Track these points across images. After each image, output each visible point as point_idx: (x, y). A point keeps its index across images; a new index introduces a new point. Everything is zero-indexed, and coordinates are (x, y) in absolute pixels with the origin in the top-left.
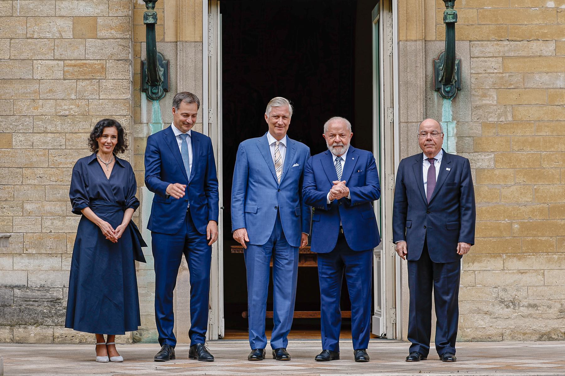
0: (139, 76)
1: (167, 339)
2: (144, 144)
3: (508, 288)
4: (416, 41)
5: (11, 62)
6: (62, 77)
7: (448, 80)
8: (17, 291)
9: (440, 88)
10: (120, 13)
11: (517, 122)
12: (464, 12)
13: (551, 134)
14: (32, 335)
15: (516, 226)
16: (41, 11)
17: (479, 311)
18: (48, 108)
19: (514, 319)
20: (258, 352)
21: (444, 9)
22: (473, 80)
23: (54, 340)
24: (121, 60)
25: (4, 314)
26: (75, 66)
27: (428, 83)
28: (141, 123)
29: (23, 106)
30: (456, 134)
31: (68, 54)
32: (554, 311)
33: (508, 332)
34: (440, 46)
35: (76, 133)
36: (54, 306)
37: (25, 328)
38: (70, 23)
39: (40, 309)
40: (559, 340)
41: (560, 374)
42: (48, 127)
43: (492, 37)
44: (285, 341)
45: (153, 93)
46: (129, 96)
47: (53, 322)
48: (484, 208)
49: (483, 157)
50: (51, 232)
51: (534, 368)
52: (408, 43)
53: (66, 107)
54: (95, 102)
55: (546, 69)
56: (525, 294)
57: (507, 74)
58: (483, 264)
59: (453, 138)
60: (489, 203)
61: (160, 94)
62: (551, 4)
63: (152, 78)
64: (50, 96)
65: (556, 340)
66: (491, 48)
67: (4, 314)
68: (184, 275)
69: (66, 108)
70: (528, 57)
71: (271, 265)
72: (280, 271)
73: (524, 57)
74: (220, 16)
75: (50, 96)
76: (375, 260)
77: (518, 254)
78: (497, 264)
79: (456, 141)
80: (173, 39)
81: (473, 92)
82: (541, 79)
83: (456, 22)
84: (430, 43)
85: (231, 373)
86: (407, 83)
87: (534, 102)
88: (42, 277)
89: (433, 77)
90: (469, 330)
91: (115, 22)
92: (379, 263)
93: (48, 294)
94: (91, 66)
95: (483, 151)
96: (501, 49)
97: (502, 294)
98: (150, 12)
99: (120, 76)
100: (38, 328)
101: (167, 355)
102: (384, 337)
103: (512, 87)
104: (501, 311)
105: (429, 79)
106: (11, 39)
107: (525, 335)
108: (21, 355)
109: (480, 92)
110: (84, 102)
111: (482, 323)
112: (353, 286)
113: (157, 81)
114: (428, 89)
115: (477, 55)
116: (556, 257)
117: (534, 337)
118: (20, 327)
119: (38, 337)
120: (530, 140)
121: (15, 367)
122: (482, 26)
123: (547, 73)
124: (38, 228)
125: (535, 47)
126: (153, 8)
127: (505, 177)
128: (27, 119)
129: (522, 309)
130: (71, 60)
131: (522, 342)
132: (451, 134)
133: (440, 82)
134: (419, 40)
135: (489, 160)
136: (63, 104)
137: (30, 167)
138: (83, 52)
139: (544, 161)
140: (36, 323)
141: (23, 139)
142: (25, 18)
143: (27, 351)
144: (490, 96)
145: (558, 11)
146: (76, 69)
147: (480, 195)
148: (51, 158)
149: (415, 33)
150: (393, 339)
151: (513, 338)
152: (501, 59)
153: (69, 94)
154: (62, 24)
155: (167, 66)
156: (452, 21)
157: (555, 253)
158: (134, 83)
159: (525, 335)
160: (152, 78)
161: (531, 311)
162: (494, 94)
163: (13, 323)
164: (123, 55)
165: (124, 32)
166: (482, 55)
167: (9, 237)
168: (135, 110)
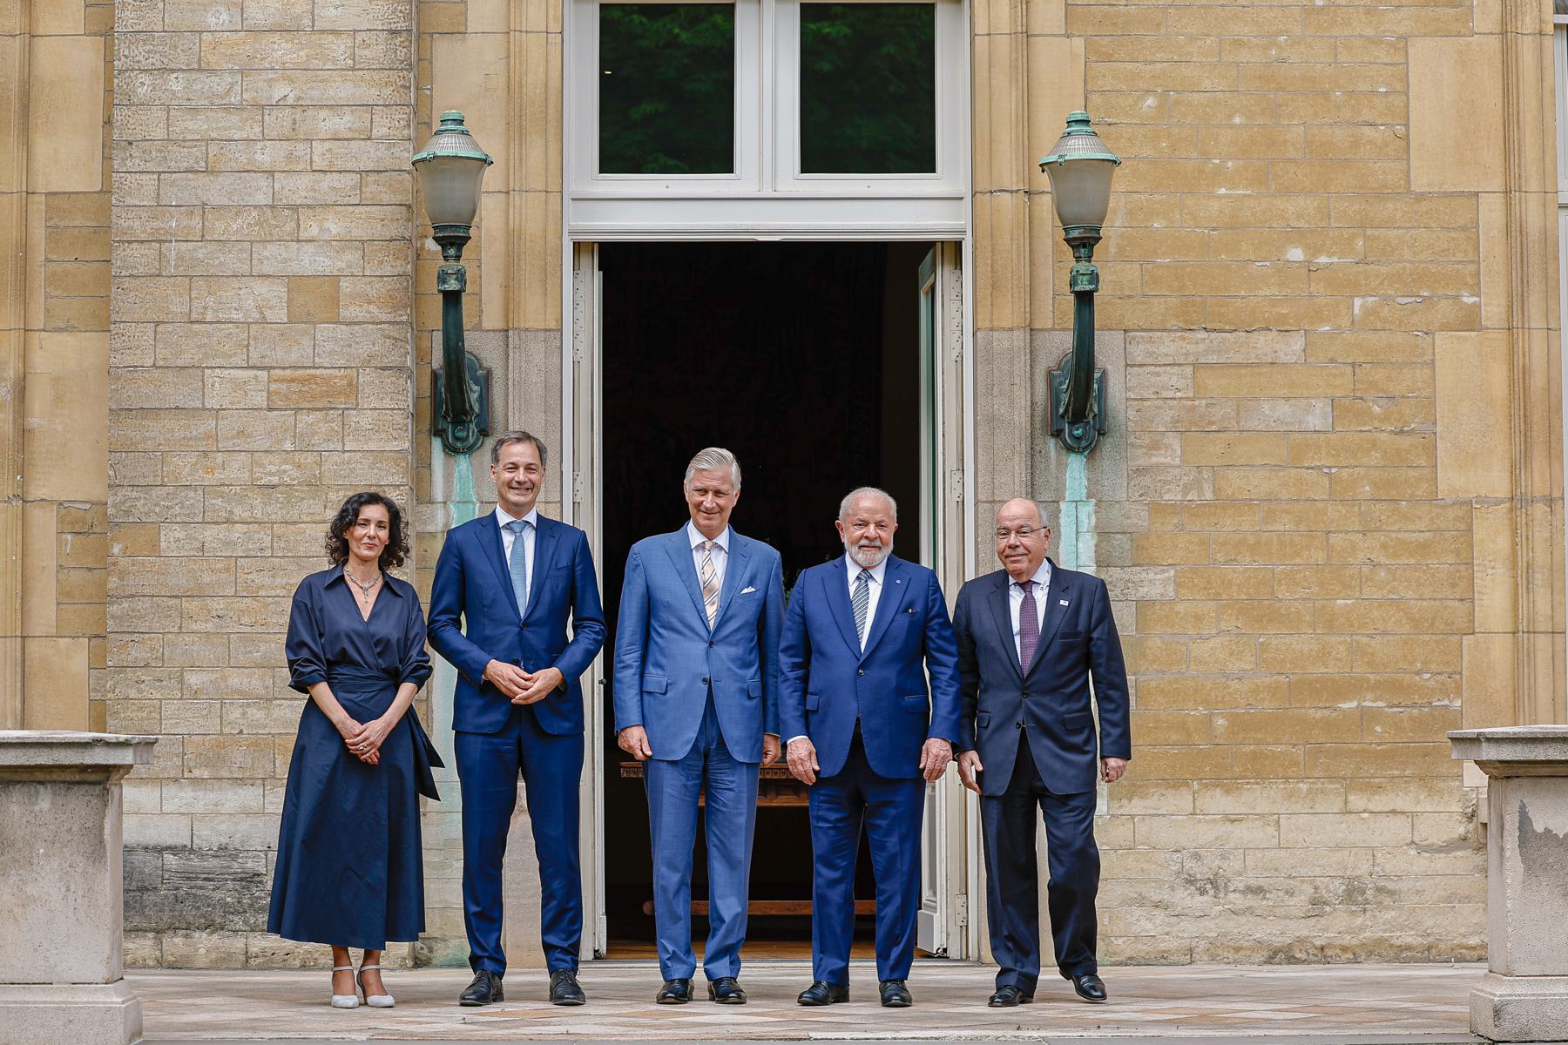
0: (428, 401)
1: (488, 960)
2: (438, 546)
3: (1202, 852)
4: (1011, 329)
5: (156, 373)
6: (264, 405)
7: (1078, 414)
8: (169, 858)
9: (1062, 431)
10: (388, 270)
11: (1224, 503)
12: (1114, 271)
13: (1293, 527)
14: (202, 951)
15: (1221, 721)
16: (221, 264)
17: (1141, 901)
18: (236, 470)
19: (1216, 917)
20: (677, 985)
21: (1072, 262)
22: (1131, 413)
23: (247, 962)
24: (390, 368)
25: (143, 907)
26: (292, 380)
27: (1038, 419)
28: (431, 502)
29: (183, 465)
30: (1096, 527)
31: (280, 355)
32: (1299, 902)
33: (1203, 944)
34: (1063, 342)
35: (294, 523)
36: (248, 889)
37: (186, 936)
38: (281, 290)
39: (217, 895)
40: (1310, 963)
41: (1312, 1033)
42: (236, 511)
43: (1172, 323)
44: (735, 963)
45: (458, 439)
46: (407, 445)
47: (246, 922)
48: (1153, 684)
49: (1151, 575)
50: (241, 732)
51: (1257, 1020)
52: (996, 334)
53: (273, 469)
54: (335, 457)
55: (1284, 392)
56: (1237, 865)
57: (1204, 402)
58: (1148, 802)
59: (1088, 536)
60: (1164, 672)
61: (471, 440)
62: (1296, 254)
63: (455, 406)
64: (240, 443)
65: (1304, 962)
66: (1169, 346)
67: (143, 907)
68: (521, 824)
69: (272, 469)
70: (1247, 365)
71: (702, 803)
72: (720, 816)
73: (1239, 365)
74: (598, 276)
75: (240, 443)
76: (928, 791)
77: (1226, 781)
78: (1181, 801)
79: (1094, 542)
80: (500, 325)
81: (1132, 439)
82: (1274, 412)
83: (1096, 290)
84: (1040, 335)
85: (622, 1030)
86: (991, 419)
87: (1259, 461)
88: (223, 827)
89: (1045, 409)
90: (1120, 941)
91: (377, 289)
92: (933, 798)
93: (236, 865)
94: (327, 380)
95: (1153, 563)
96: (1192, 348)
97: (1190, 865)
98: (452, 267)
99: (388, 403)
100: (215, 937)
101: (487, 991)
102: (943, 955)
103: (1214, 428)
104: (1188, 902)
105: (1039, 411)
106: (157, 323)
107: (1237, 951)
108: (178, 993)
109: (1147, 441)
110: (311, 458)
111: (1149, 926)
112: (882, 847)
113: (465, 413)
114: (1038, 433)
115: (1139, 360)
116: (1303, 787)
117: (1258, 957)
118: (176, 935)
119: (214, 956)
120: (1251, 540)
121: (166, 1018)
122: (1156, 301)
123: (1288, 399)
124: (213, 725)
125: (1264, 345)
126: (458, 258)
127: (1198, 618)
128: (192, 494)
129: (1232, 896)
130: (284, 368)
131: (1232, 967)
132: (1084, 527)
133: (1062, 416)
134: (1019, 328)
135: (1165, 582)
136: (266, 462)
137: (198, 594)
138: (310, 351)
139: (1280, 584)
140: (210, 926)
141: (181, 535)
142: (187, 280)
143: (191, 985)
144: (1167, 447)
145: (1310, 269)
146: (295, 387)
147: (1144, 656)
148: (242, 577)
149: (1010, 313)
150: (961, 960)
151: (1213, 958)
152: (1189, 370)
153: (279, 441)
154: (264, 291)
155: (486, 381)
156: (1088, 288)
157: (1302, 779)
158: (416, 417)
159: (1237, 951)
160: (455, 406)
161: (1251, 900)
162: (1174, 442)
163: (162, 925)
164: (394, 359)
165: (395, 308)
166: (1149, 361)
167: (152, 744)
168: (418, 474)
